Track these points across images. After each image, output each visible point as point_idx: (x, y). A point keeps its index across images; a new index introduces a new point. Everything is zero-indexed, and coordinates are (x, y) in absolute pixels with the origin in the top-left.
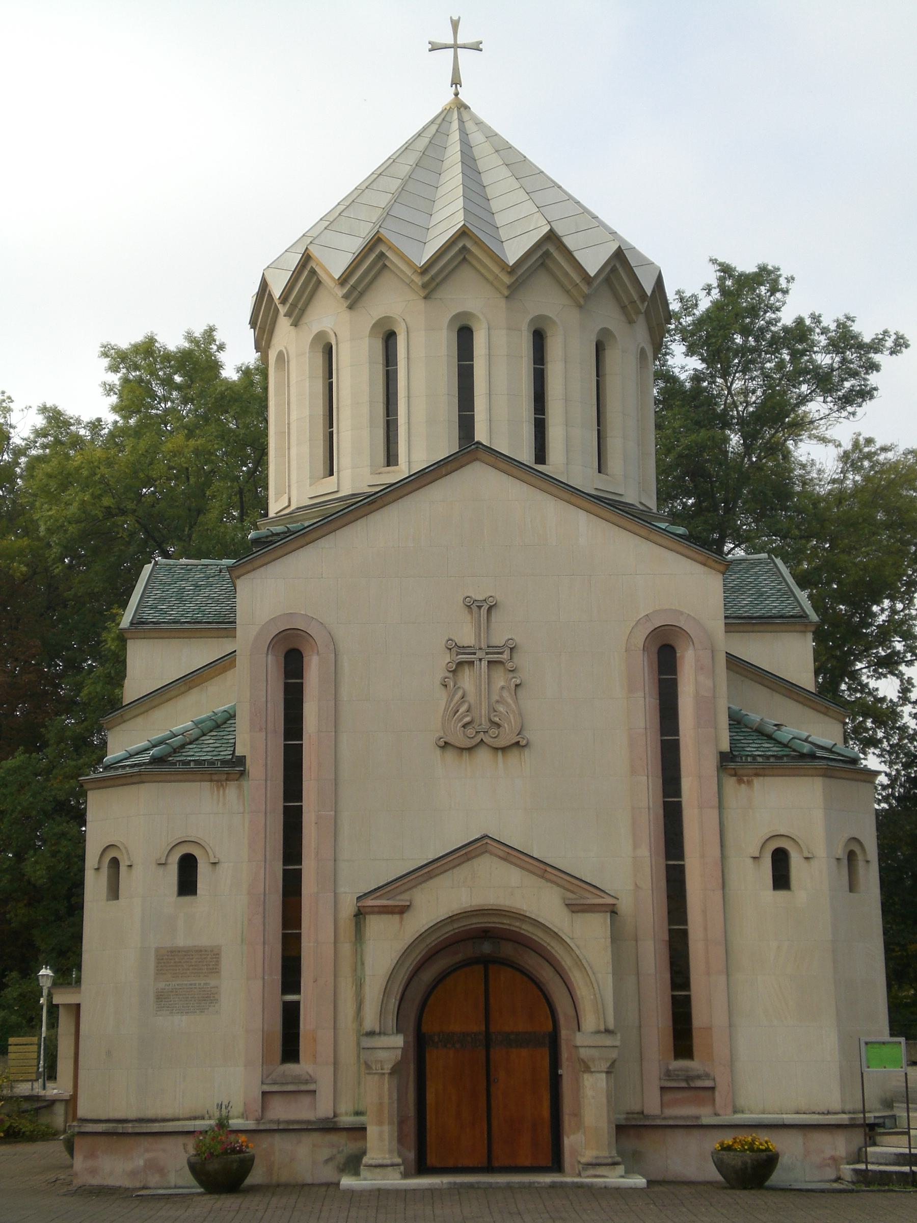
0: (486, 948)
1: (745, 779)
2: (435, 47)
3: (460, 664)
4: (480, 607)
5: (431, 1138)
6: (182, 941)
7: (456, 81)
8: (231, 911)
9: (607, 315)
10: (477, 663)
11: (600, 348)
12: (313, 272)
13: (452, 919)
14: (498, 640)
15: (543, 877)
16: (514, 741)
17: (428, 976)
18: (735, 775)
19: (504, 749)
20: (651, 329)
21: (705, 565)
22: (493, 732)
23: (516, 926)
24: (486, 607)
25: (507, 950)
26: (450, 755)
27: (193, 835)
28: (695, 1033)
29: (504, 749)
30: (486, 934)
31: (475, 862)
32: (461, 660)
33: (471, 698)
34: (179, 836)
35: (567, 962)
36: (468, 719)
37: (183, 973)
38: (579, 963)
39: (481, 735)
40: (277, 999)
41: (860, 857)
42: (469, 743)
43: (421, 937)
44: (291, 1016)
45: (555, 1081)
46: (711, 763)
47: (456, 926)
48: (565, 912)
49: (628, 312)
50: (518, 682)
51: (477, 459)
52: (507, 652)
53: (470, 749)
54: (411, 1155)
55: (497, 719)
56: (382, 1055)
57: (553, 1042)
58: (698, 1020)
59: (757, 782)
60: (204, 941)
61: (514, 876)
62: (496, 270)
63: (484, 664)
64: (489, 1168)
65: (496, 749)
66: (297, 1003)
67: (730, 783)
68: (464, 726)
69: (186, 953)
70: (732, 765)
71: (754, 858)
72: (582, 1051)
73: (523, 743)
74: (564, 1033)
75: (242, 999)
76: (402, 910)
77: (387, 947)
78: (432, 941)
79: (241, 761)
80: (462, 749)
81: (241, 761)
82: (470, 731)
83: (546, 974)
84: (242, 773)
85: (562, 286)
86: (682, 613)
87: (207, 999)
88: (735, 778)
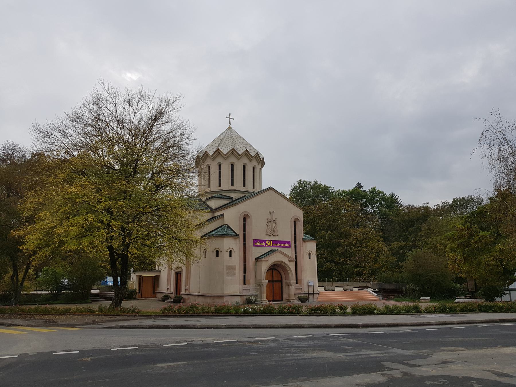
2: (227, 117)
7: (230, 124)
8: (236, 260)
32: (269, 221)
57: (281, 281)
61: (282, 256)
69: (231, 266)
76: (267, 261)
87: (234, 274)
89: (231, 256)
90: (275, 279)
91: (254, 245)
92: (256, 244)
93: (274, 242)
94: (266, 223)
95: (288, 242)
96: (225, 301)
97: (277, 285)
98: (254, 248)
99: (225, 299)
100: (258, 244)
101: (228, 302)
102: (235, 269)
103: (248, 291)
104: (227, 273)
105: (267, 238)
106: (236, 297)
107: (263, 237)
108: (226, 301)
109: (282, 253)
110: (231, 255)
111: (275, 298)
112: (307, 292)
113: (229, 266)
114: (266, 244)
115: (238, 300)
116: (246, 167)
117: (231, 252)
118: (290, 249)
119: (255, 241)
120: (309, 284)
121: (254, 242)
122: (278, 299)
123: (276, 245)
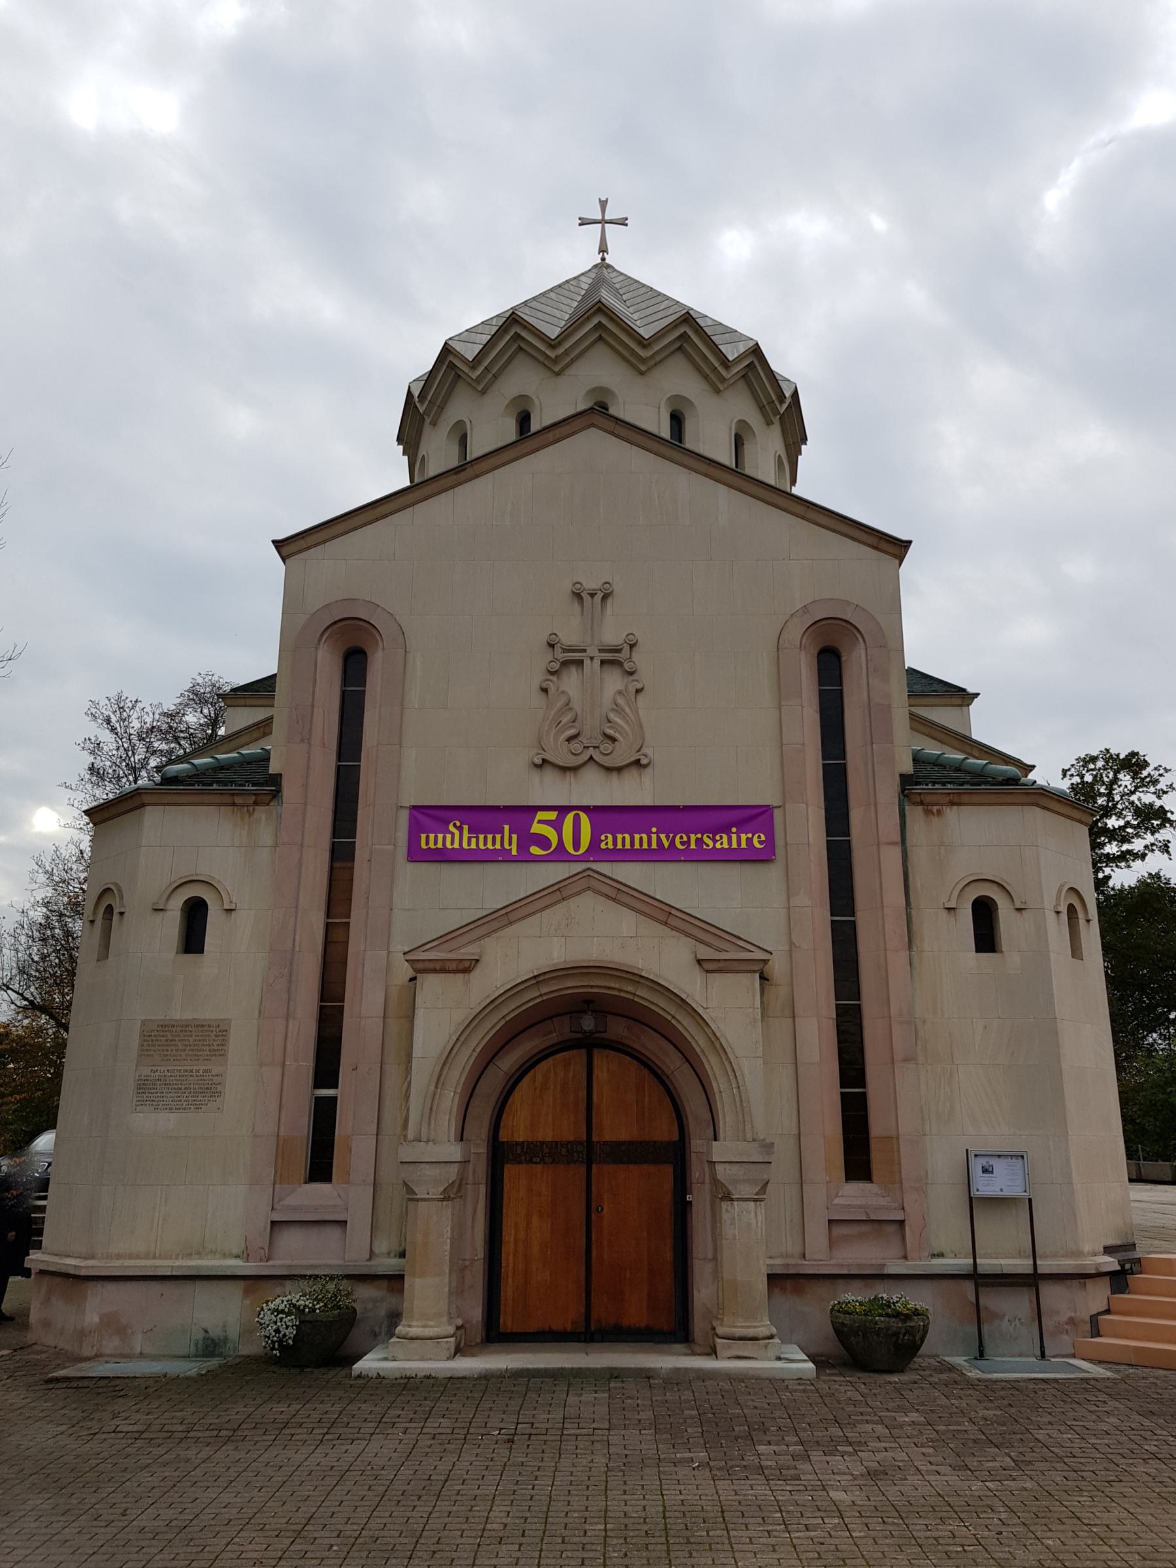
0: (588, 1023)
1: (935, 809)
3: (565, 664)
4: (592, 595)
5: (508, 1290)
6: (178, 1014)
10: (587, 662)
13: (538, 979)
14: (612, 635)
15: (666, 924)
16: (633, 759)
17: (508, 1062)
18: (922, 803)
19: (619, 770)
20: (787, 446)
21: (876, 548)
22: (607, 747)
24: (600, 595)
25: (618, 1029)
26: (550, 775)
27: (203, 871)
28: (875, 1146)
29: (619, 770)
30: (588, 1004)
31: (572, 903)
33: (576, 705)
34: (185, 873)
35: (699, 1042)
36: (572, 732)
37: (182, 1053)
38: (714, 1041)
41: (1081, 915)
43: (494, 1004)
44: (324, 1115)
45: (682, 1210)
46: (889, 792)
47: (544, 991)
48: (697, 974)
50: (639, 686)
51: (592, 425)
52: (626, 648)
53: (574, 769)
54: (476, 1313)
55: (610, 732)
56: (430, 1172)
58: (877, 1128)
59: (951, 813)
60: (207, 1014)
61: (626, 922)
63: (597, 662)
64: (588, 1333)
66: (334, 1100)
67: (915, 814)
68: (569, 740)
69: (184, 1027)
71: (949, 909)
72: (719, 1167)
73: (644, 761)
74: (696, 1144)
75: (257, 1090)
76: (466, 967)
77: (443, 1018)
78: (510, 1010)
79: (276, 780)
80: (564, 769)
81: (276, 780)
82: (576, 746)
83: (672, 1063)
84: (276, 794)
85: (699, 370)
86: (848, 603)
87: (208, 1090)
88: (920, 808)
89: (193, 940)
90: (615, 1128)
91: (416, 854)
92: (431, 841)
93: (606, 816)
94: (538, 678)
95: (756, 817)
96: (92, 1317)
97: (629, 1192)
99: (96, 1306)
100: (455, 838)
101: (122, 1331)
102: (220, 1052)
103: (334, 1233)
104: (143, 1087)
105: (549, 790)
106: (201, 1292)
108: (112, 1324)
109: (621, 894)
110: (193, 940)
112: (963, 1263)
113: (164, 1026)
114: (528, 839)
115: (222, 1313)
117: (195, 912)
118: (771, 874)
119: (428, 817)
120: (984, 1187)
121: (415, 829)
122: (636, 1313)
123: (623, 840)
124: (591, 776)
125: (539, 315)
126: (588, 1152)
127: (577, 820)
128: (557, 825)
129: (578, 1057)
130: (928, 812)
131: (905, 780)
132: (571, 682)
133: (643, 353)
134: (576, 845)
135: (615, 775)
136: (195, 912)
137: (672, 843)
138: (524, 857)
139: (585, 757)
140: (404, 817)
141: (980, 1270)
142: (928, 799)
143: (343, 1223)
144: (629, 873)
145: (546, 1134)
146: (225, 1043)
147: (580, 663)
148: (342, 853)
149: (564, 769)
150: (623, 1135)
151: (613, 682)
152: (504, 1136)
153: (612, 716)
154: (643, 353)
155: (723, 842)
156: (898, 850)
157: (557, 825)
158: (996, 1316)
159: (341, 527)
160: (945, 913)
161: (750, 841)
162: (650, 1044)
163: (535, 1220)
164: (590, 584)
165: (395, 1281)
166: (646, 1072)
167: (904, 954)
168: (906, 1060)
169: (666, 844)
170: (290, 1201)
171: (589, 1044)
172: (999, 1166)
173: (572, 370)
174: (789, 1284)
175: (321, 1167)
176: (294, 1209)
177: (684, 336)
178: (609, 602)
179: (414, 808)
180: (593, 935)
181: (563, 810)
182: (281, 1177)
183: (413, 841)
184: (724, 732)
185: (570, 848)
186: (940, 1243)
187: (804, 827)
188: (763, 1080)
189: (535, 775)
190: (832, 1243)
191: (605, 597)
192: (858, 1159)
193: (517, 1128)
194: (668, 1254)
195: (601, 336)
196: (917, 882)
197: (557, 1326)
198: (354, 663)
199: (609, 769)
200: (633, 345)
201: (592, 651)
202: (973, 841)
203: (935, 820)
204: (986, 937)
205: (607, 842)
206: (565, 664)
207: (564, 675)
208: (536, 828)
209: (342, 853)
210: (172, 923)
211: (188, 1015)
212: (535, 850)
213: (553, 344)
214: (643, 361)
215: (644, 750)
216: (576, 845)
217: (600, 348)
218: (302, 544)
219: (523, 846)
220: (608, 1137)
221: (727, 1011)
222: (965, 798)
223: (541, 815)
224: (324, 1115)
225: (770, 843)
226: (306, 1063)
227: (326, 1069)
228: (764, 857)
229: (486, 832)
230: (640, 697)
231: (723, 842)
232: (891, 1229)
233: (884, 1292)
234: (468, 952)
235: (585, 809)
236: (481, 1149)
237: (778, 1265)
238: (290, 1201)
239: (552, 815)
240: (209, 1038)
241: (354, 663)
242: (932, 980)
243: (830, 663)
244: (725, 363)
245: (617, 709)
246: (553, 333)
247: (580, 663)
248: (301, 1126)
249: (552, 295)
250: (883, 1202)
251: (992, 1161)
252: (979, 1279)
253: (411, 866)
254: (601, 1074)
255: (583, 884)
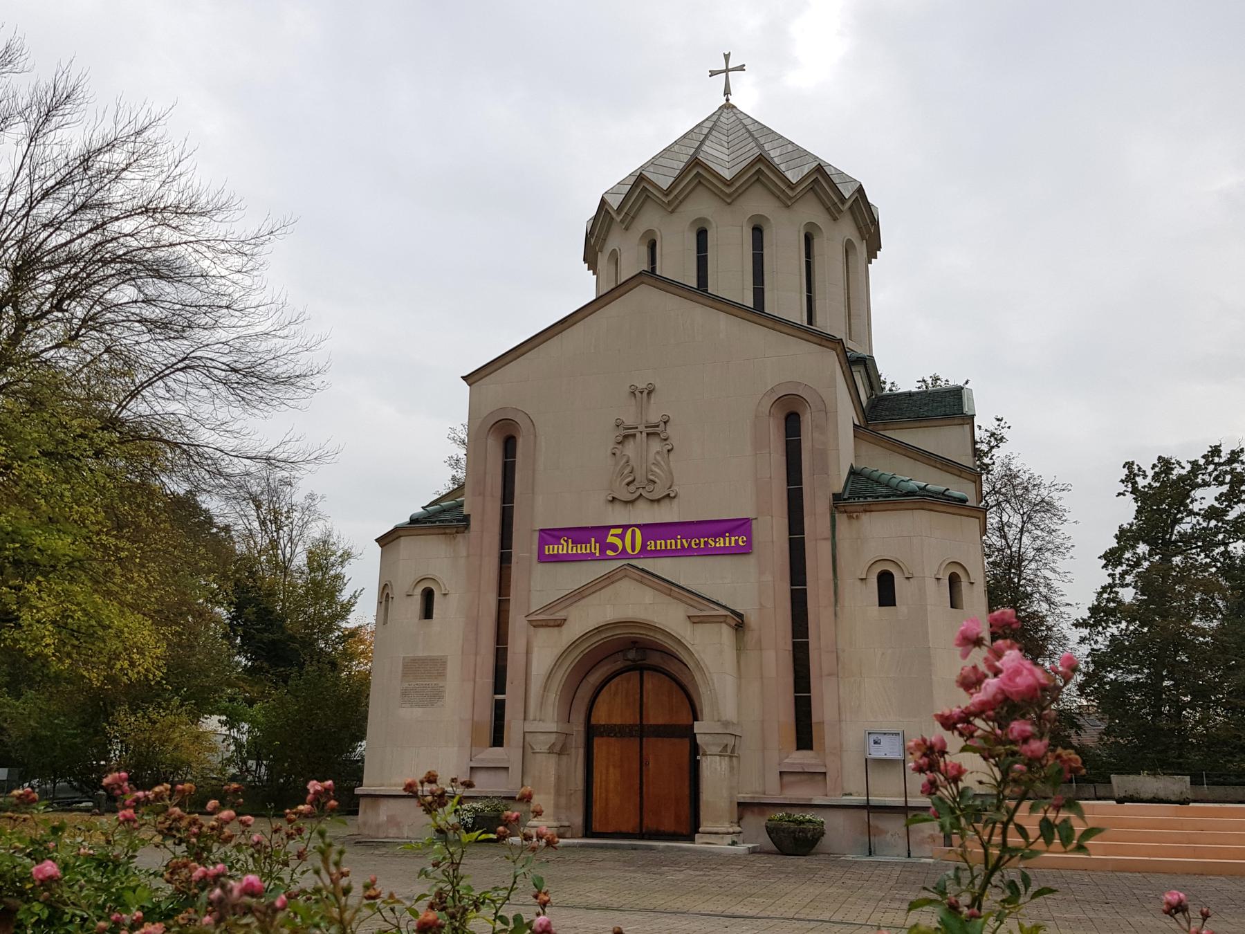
0: (631, 655)
3: (626, 437)
5: (597, 809)
6: (421, 653)
9: (809, 212)
10: (638, 435)
11: (809, 239)
12: (607, 212)
14: (654, 418)
17: (595, 678)
19: (658, 501)
23: (660, 638)
25: (655, 659)
26: (618, 507)
27: (431, 573)
29: (658, 501)
30: (635, 644)
33: (632, 463)
34: (422, 574)
39: (640, 491)
40: (486, 697)
41: (964, 579)
42: (630, 497)
44: (499, 709)
49: (833, 212)
52: (662, 425)
53: (632, 502)
55: (652, 478)
59: (865, 518)
60: (436, 653)
62: (720, 185)
63: (644, 435)
65: (652, 501)
66: (504, 701)
67: (842, 519)
68: (628, 484)
69: (424, 661)
70: (842, 503)
75: (462, 695)
79: (467, 518)
80: (626, 502)
84: (467, 527)
85: (773, 194)
89: (428, 613)
90: (656, 717)
91: (543, 558)
92: (550, 550)
93: (650, 530)
95: (741, 526)
97: (664, 754)
98: (541, 568)
102: (442, 674)
103: (503, 774)
104: (405, 693)
105: (619, 516)
107: (594, 513)
111: (650, 823)
112: (859, 799)
113: (415, 660)
114: (605, 546)
116: (817, 244)
117: (428, 596)
119: (550, 535)
120: (877, 753)
121: (542, 543)
122: (668, 825)
123: (661, 544)
124: (641, 505)
125: (661, 170)
126: (641, 731)
127: (633, 532)
128: (622, 537)
129: (635, 675)
130: (850, 518)
131: (837, 497)
132: (630, 449)
133: (728, 191)
134: (633, 549)
135: (656, 505)
136: (428, 596)
137: (690, 545)
138: (604, 558)
139: (637, 494)
140: (536, 535)
141: (871, 803)
142: (849, 509)
143: (507, 768)
144: (663, 567)
145: (617, 720)
146: (445, 669)
147: (634, 436)
148: (505, 559)
149: (626, 502)
150: (661, 721)
151: (655, 445)
152: (593, 721)
153: (653, 467)
154: (728, 191)
155: (720, 543)
156: (828, 545)
157: (622, 537)
158: (882, 832)
159: (499, 364)
160: (859, 582)
161: (736, 541)
162: (673, 668)
163: (611, 770)
164: (642, 385)
165: (526, 798)
166: (675, 685)
167: (832, 609)
168: (830, 675)
169: (686, 545)
170: (480, 756)
171: (640, 668)
172: (884, 739)
173: (681, 209)
174: (756, 809)
175: (498, 739)
176: (483, 760)
177: (759, 171)
178: (653, 395)
179: (542, 530)
180: (631, 604)
181: (625, 528)
182: (474, 743)
183: (541, 550)
184: (725, 473)
185: (629, 551)
186: (850, 787)
187: (772, 532)
188: (734, 691)
189: (610, 507)
190: (782, 786)
191: (649, 393)
192: (804, 737)
193: (601, 716)
194: (687, 791)
195: (699, 181)
196: (841, 563)
197: (624, 829)
198: (509, 445)
199: (652, 501)
200: (720, 185)
201: (641, 428)
202: (882, 535)
203: (854, 521)
204: (887, 594)
205: (651, 546)
206: (626, 437)
207: (626, 443)
208: (610, 539)
209: (505, 559)
210: (417, 602)
211: (426, 654)
212: (609, 553)
213: (667, 193)
214: (729, 195)
215: (674, 488)
216: (633, 549)
217: (700, 188)
218: (477, 377)
219: (602, 551)
220: (652, 722)
221: (709, 651)
222: (873, 507)
223: (613, 531)
224: (499, 708)
225: (749, 543)
226: (487, 680)
227: (499, 684)
228: (745, 551)
229: (581, 543)
230: (672, 454)
231: (720, 543)
232: (820, 778)
233: (798, 815)
234: (560, 615)
235: (638, 526)
236: (578, 728)
237: (745, 797)
238: (480, 756)
239: (619, 531)
240: (436, 666)
241: (509, 445)
242: (852, 625)
243: (792, 423)
244: (791, 186)
245: (656, 464)
246: (665, 183)
247: (634, 436)
248: (487, 715)
249: (663, 161)
250: (813, 761)
251: (880, 737)
252: (869, 808)
253: (540, 566)
254: (648, 685)
255: (622, 574)
